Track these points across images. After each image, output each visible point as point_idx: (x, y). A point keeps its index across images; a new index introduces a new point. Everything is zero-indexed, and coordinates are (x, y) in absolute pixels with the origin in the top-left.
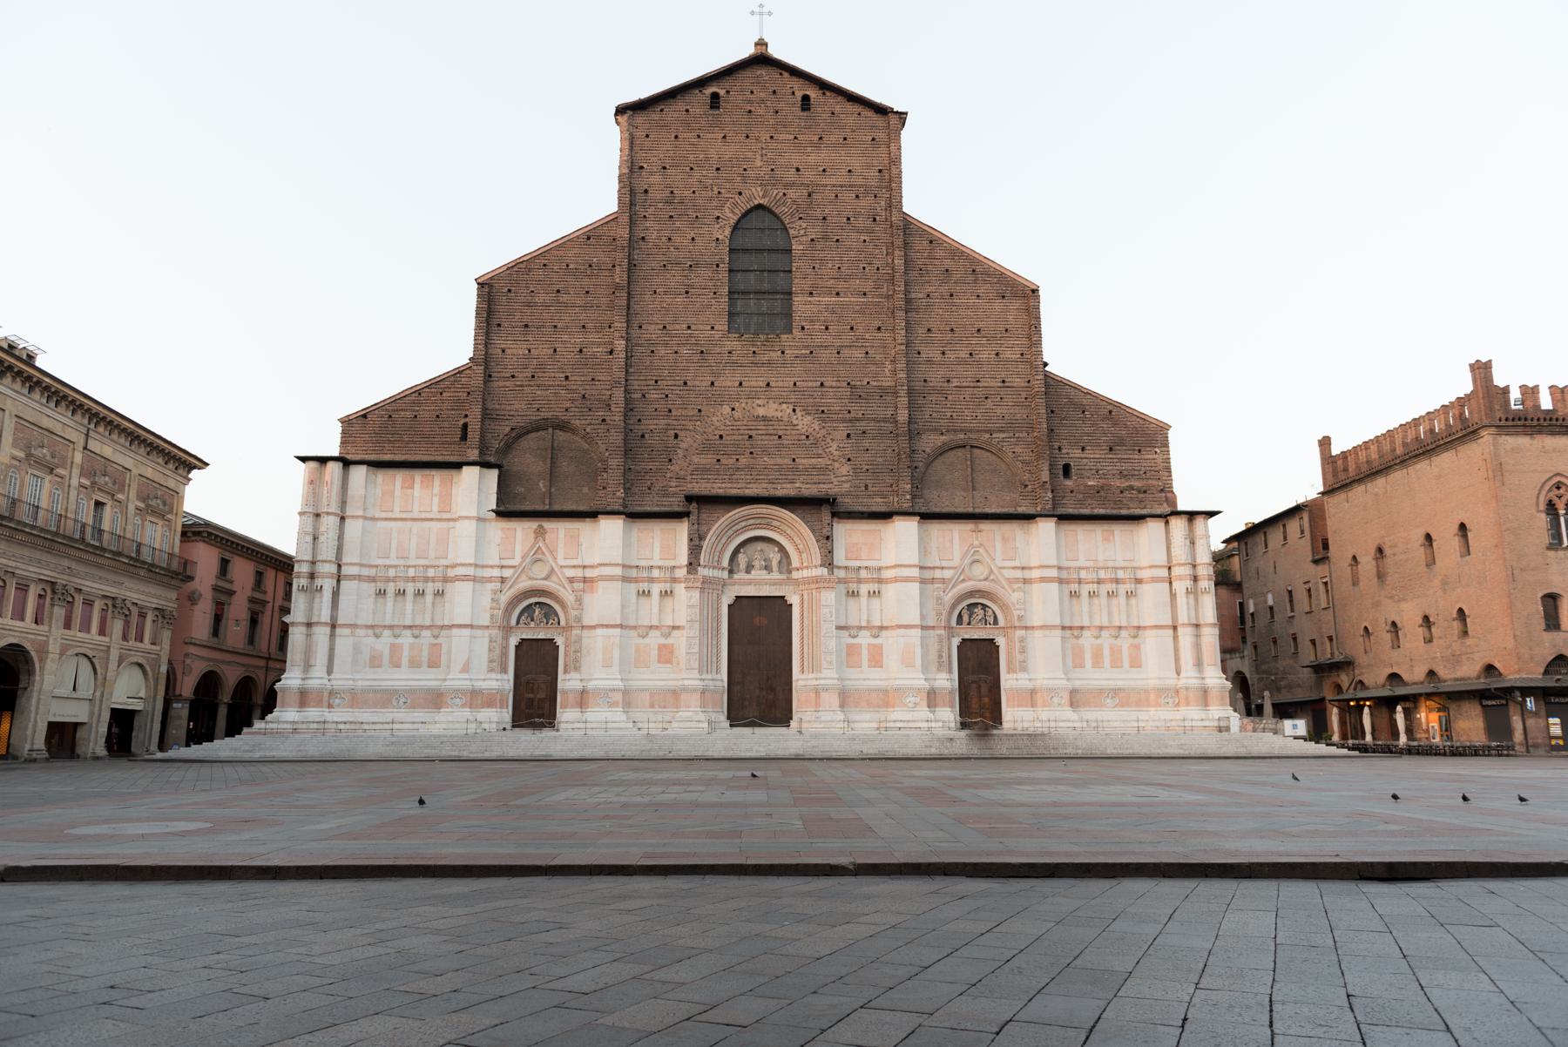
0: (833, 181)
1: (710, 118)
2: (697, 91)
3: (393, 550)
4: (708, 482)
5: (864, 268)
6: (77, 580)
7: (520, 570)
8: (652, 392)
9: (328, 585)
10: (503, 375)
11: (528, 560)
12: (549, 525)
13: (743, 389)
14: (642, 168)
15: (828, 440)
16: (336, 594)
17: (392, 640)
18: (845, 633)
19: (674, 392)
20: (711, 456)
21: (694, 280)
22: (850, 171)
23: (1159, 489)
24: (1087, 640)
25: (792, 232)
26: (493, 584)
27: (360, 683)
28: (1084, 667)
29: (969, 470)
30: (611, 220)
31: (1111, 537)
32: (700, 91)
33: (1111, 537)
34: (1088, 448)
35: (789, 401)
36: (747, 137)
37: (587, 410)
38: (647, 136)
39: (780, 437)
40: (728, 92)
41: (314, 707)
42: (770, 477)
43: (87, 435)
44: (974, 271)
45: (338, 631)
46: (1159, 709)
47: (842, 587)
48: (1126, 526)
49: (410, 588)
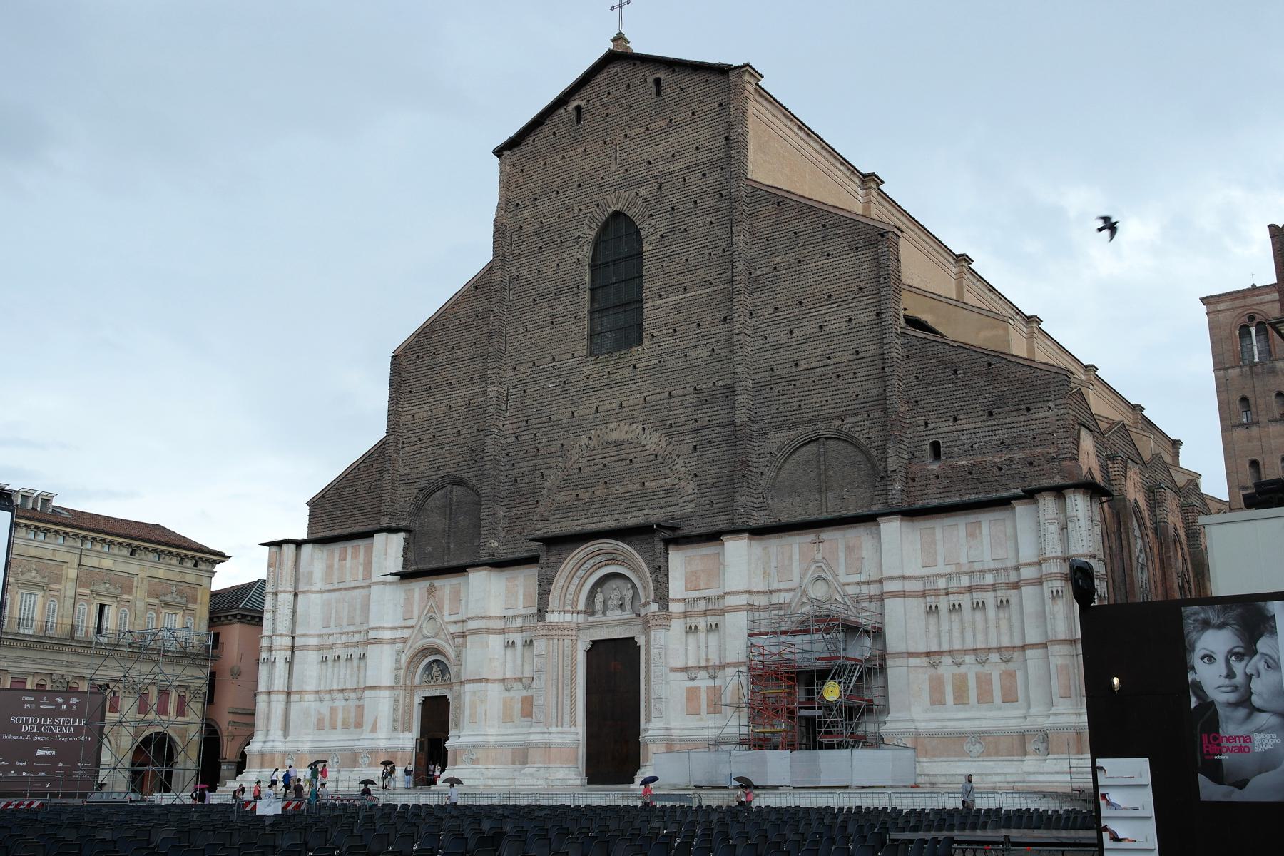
0: (682, 165)
1: (573, 135)
2: (562, 111)
3: (333, 619)
4: (567, 521)
5: (710, 253)
6: (77, 670)
7: (417, 628)
8: (523, 433)
9: (281, 656)
10: (413, 439)
11: (422, 618)
12: (438, 582)
13: (598, 415)
14: (518, 204)
15: (674, 457)
16: (290, 663)
17: (330, 704)
18: (683, 675)
19: (541, 430)
20: (569, 492)
21: (559, 309)
22: (697, 148)
23: (1049, 456)
24: (947, 669)
25: (643, 233)
26: (397, 645)
27: (309, 744)
28: (945, 704)
29: (823, 467)
30: (489, 269)
31: (977, 531)
32: (565, 109)
33: (977, 531)
34: (961, 417)
35: (641, 419)
36: (605, 143)
37: (473, 461)
38: (522, 170)
39: (631, 461)
40: (588, 101)
41: (267, 768)
42: (622, 507)
43: (81, 554)
44: (824, 226)
45: (294, 698)
46: (1028, 757)
47: (677, 626)
48: (994, 511)
49: (342, 653)
